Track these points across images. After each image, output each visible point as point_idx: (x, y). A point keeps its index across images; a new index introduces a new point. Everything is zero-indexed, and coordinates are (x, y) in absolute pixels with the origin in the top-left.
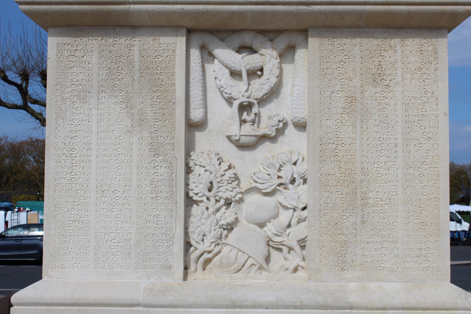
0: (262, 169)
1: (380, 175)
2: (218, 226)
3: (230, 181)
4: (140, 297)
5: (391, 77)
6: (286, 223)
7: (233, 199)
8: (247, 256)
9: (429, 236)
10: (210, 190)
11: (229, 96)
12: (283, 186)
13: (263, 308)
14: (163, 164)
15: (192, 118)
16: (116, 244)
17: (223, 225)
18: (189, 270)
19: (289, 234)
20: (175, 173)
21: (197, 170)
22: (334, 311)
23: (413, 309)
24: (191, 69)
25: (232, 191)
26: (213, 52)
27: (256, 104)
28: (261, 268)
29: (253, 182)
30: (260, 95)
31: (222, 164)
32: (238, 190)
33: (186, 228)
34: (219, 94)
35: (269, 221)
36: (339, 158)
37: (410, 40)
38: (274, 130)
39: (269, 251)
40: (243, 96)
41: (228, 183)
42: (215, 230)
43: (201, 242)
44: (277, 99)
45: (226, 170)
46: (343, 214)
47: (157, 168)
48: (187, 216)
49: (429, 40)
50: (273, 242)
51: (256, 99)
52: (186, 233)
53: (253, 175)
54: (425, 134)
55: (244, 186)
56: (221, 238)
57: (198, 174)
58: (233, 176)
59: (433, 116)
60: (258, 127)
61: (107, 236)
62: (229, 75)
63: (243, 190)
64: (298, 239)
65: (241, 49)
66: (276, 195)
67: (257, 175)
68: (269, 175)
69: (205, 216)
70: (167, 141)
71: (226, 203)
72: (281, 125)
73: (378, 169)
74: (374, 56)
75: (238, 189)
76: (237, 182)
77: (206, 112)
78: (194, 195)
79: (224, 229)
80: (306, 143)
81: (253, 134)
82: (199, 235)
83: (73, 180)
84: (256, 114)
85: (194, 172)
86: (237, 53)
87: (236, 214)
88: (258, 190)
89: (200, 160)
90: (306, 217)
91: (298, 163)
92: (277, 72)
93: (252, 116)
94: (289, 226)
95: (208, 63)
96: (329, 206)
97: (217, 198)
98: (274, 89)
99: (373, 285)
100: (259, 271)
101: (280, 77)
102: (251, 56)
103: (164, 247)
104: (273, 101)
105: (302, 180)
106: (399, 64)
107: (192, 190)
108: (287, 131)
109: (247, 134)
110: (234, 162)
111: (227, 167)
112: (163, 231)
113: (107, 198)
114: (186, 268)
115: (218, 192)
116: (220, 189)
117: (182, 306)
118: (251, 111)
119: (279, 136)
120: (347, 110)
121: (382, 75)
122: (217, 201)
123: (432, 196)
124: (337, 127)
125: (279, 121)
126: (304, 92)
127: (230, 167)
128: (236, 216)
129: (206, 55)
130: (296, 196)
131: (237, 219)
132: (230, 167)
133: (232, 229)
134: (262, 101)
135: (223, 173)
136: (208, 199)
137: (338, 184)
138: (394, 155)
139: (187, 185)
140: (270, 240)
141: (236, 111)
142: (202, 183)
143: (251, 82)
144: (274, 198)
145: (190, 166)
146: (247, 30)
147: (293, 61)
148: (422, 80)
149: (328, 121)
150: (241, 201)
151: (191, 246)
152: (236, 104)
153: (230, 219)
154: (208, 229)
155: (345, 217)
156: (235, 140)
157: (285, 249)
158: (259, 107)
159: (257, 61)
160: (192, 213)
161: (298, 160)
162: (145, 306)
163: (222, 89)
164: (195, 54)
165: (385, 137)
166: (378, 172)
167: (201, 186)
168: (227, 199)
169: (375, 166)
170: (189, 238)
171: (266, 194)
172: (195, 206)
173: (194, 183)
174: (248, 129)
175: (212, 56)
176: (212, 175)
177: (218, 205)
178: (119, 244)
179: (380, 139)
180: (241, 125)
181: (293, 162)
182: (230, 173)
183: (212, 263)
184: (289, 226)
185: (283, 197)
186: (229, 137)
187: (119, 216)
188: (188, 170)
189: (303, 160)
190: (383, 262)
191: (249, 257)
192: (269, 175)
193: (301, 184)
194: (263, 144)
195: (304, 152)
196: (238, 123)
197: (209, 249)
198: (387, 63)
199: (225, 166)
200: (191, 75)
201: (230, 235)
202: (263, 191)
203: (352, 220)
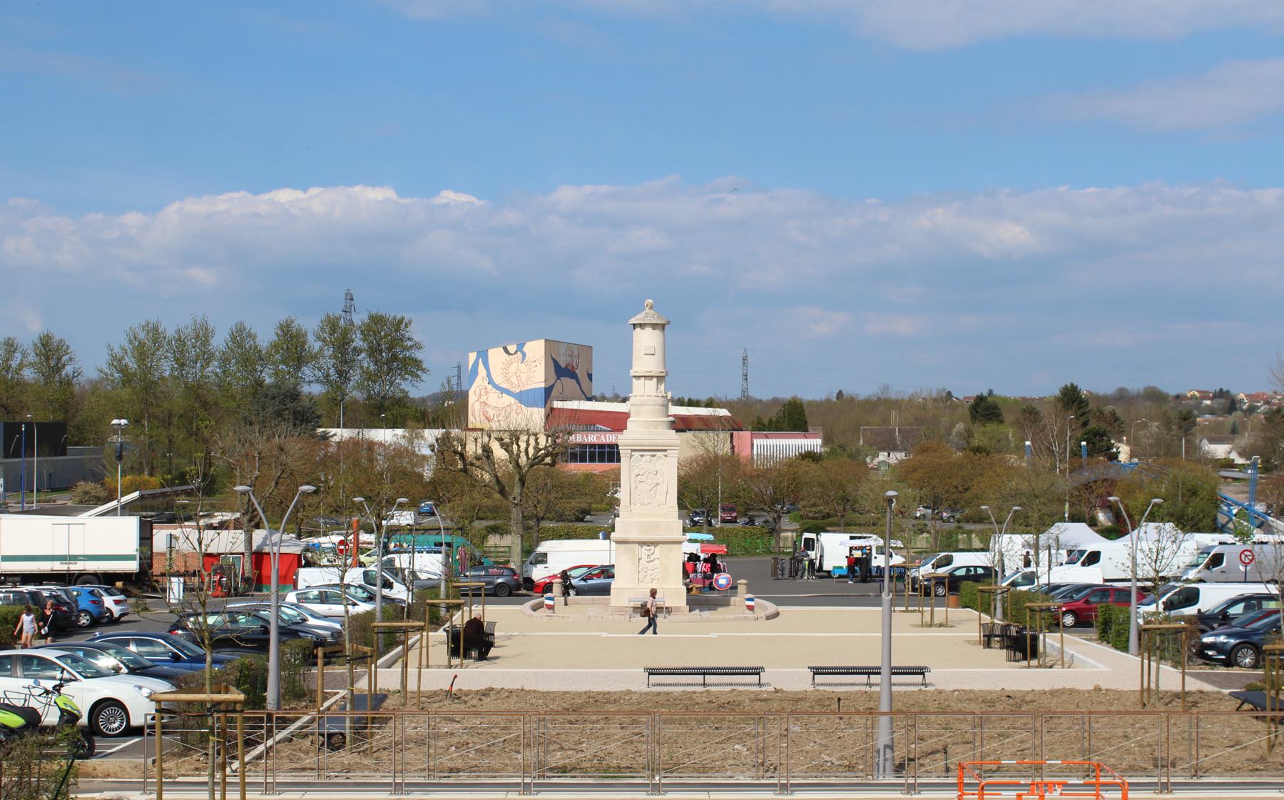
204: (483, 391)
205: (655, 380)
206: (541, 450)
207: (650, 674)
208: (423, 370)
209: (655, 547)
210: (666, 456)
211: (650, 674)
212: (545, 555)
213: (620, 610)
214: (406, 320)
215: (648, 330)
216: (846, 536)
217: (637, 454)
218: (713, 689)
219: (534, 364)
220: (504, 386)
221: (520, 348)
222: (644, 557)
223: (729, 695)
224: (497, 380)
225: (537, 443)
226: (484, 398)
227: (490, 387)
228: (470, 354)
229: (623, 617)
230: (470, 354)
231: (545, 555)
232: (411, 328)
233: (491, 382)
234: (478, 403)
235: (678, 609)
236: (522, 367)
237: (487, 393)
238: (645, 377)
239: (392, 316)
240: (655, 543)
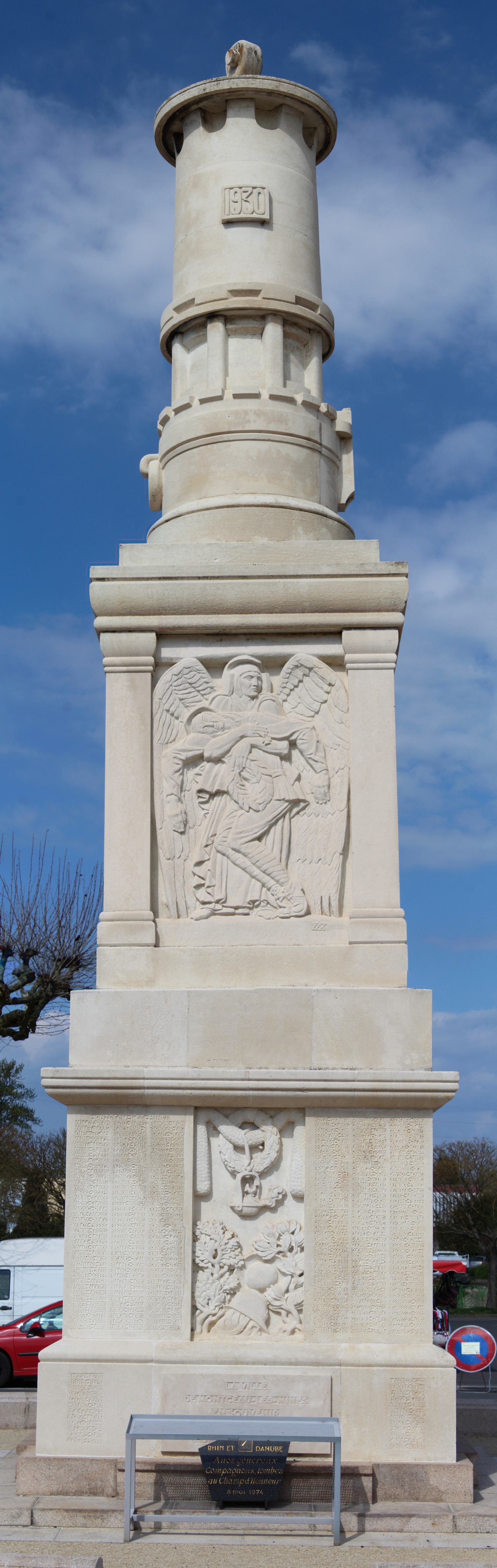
0: (263, 1238)
1: (370, 1245)
2: (222, 1291)
3: (233, 1249)
4: (153, 1354)
5: (381, 1154)
6: (284, 1289)
7: (236, 1266)
8: (249, 1319)
9: (413, 1301)
10: (214, 1257)
11: (233, 1169)
12: (282, 1254)
13: (262, 1365)
14: (172, 1233)
15: (198, 1190)
16: (129, 1306)
17: (226, 1290)
18: (196, 1332)
19: (287, 1299)
20: (183, 1242)
21: (203, 1239)
22: (325, 1367)
23: (395, 1366)
24: (198, 1144)
25: (235, 1258)
26: (218, 1128)
27: (258, 1177)
28: (261, 1330)
29: (255, 1250)
30: (261, 1168)
31: (226, 1232)
32: (240, 1257)
33: (193, 1293)
34: (223, 1166)
35: (269, 1287)
36: (332, 1229)
37: (399, 1119)
38: (274, 1201)
39: (268, 1314)
40: (246, 1170)
41: (231, 1251)
42: (219, 1294)
43: (207, 1306)
44: (277, 1171)
45: (230, 1239)
46: (335, 1280)
47: (167, 1237)
48: (194, 1281)
49: (416, 1119)
50: (272, 1305)
51: (258, 1172)
52: (193, 1297)
53: (254, 1243)
54: (411, 1206)
55: (246, 1253)
56: (224, 1302)
57: (203, 1243)
58: (236, 1244)
59: (419, 1190)
60: (259, 1198)
61: (121, 1299)
62: (233, 1149)
63: (245, 1258)
64: (295, 1303)
65: (242, 1126)
66: (276, 1262)
67: (258, 1244)
68: (269, 1243)
69: (210, 1281)
70: (176, 1212)
71: (229, 1269)
72: (280, 1196)
73: (368, 1239)
74: (365, 1134)
75: (240, 1256)
76: (239, 1249)
77: (211, 1184)
78: (200, 1262)
79: (227, 1294)
80: (303, 1213)
81: (255, 1205)
82: (204, 1299)
83: (91, 1247)
84: (257, 1187)
85: (200, 1241)
86: (240, 1129)
87: (238, 1279)
88: (259, 1258)
89: (206, 1229)
90: (303, 1283)
91: (296, 1233)
92: (277, 1147)
93: (254, 1189)
94: (287, 1291)
95: (213, 1136)
96: (323, 1273)
97: (221, 1265)
98: (274, 1163)
99: (362, 1346)
100: (259, 1333)
101: (280, 1152)
102: (253, 1131)
103: (173, 1310)
104: (273, 1173)
105: (299, 1249)
106: (388, 1142)
107: (198, 1257)
108: (286, 1202)
109: (249, 1205)
110: (237, 1231)
111: (231, 1236)
112: (173, 1295)
113: (121, 1264)
114: (193, 1330)
115: (222, 1259)
116: (224, 1256)
117: (190, 1362)
118: (253, 1183)
119: (279, 1207)
120: (340, 1185)
121: (372, 1152)
122: (221, 1267)
123: (416, 1264)
124: (330, 1200)
125: (279, 1193)
126: (301, 1167)
127: (233, 1236)
128: (238, 1282)
129: (211, 1129)
130: (294, 1263)
131: (239, 1285)
132: (233, 1236)
133: (235, 1293)
134: (263, 1174)
135: (227, 1241)
136: (213, 1265)
137: (332, 1253)
138: (383, 1226)
139: (194, 1252)
140: (270, 1304)
141: (239, 1183)
142: (207, 1251)
143: (253, 1156)
144: (273, 1264)
145: (197, 1234)
146: (249, 1108)
147: (292, 1136)
148: (408, 1157)
149: (323, 1194)
150: (243, 1267)
151: (197, 1309)
152: (239, 1177)
153: (233, 1285)
154: (213, 1293)
155: (337, 1283)
156: (238, 1211)
157: (284, 1313)
158: (260, 1179)
159: (259, 1136)
160: (198, 1278)
161: (295, 1229)
162: (158, 1362)
163: (226, 1163)
165: (374, 1209)
166: (367, 1242)
167: (207, 1253)
168: (230, 1266)
169: (365, 1236)
170: (195, 1301)
171: (266, 1261)
172: (201, 1272)
173: (200, 1250)
174: (250, 1200)
175: (215, 1129)
176: (217, 1243)
177: (222, 1271)
178: (132, 1307)
179: (370, 1212)
180: (243, 1196)
181: (291, 1232)
182: (233, 1242)
183: (216, 1325)
184: (287, 1291)
185: (282, 1264)
186: (232, 1208)
187: (132, 1281)
188: (195, 1239)
189: (300, 1229)
190: (372, 1324)
191: (251, 1319)
192: (269, 1243)
193: (299, 1252)
194: (264, 1213)
195: (302, 1222)
196: (241, 1195)
197: (214, 1312)
198: (377, 1141)
199: (228, 1235)
200: (198, 1150)
201: (232, 1299)
202: (263, 1258)
203: (344, 1286)
209: (286, 1129)
210: (336, 663)
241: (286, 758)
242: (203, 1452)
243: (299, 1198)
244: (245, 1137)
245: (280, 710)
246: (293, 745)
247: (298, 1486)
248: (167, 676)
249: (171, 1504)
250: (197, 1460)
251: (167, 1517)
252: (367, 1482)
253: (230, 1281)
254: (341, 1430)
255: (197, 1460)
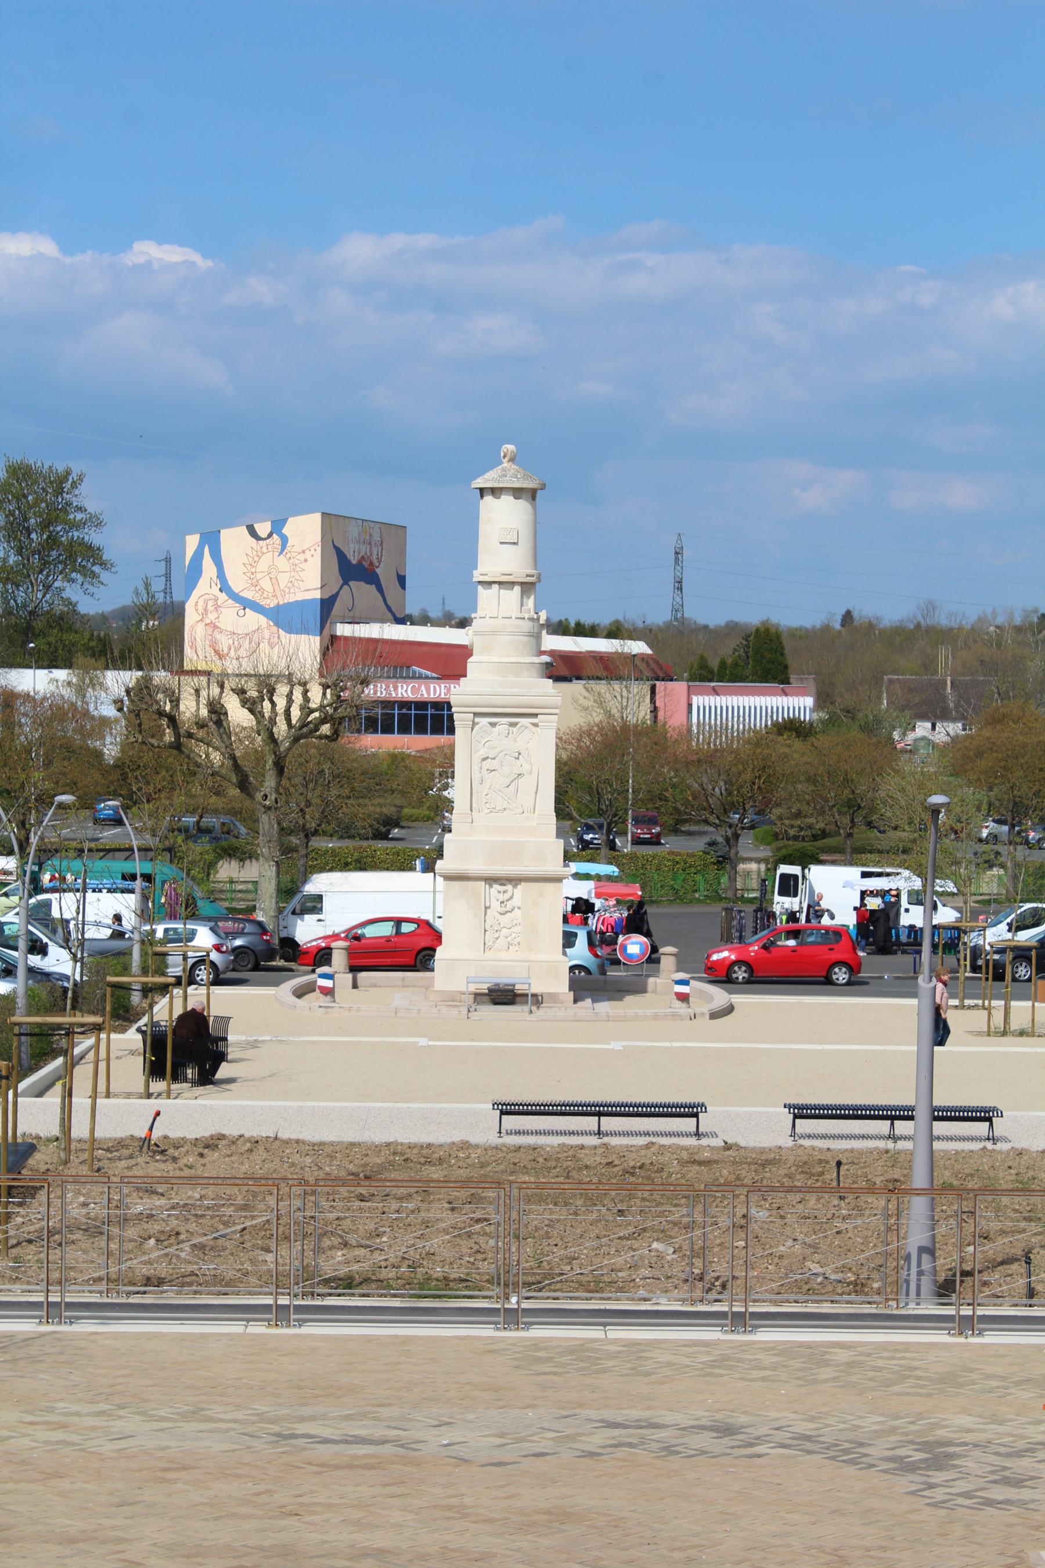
21: (487, 921)
134: (507, 901)
164: (487, 886)
204: (210, 603)
205: (517, 589)
206: (312, 711)
207: (502, 1113)
208: (103, 564)
209: (515, 886)
210: (536, 725)
211: (502, 1113)
212: (319, 898)
213: (451, 999)
214: (74, 476)
215: (507, 499)
216: (855, 872)
217: (484, 721)
218: (614, 1141)
219: (302, 557)
220: (248, 595)
221: (278, 527)
222: (495, 905)
223: (643, 1152)
224: (237, 585)
225: (306, 699)
226: (212, 617)
227: (223, 597)
228: (188, 538)
229: (455, 1011)
230: (188, 538)
231: (319, 898)
232: (83, 489)
233: (225, 588)
234: (201, 625)
235: (554, 997)
236: (282, 562)
237: (217, 607)
238: (500, 583)
239: (46, 466)
240: (515, 881)
241: (518, 758)
242: (489, 989)
243: (519, 908)
244: (501, 888)
245: (515, 741)
246: (520, 754)
247: (518, 999)
248: (477, 728)
249: (478, 1004)
250: (487, 991)
251: (478, 1007)
252: (540, 998)
253: (496, 935)
254: (532, 981)
255: (487, 991)
